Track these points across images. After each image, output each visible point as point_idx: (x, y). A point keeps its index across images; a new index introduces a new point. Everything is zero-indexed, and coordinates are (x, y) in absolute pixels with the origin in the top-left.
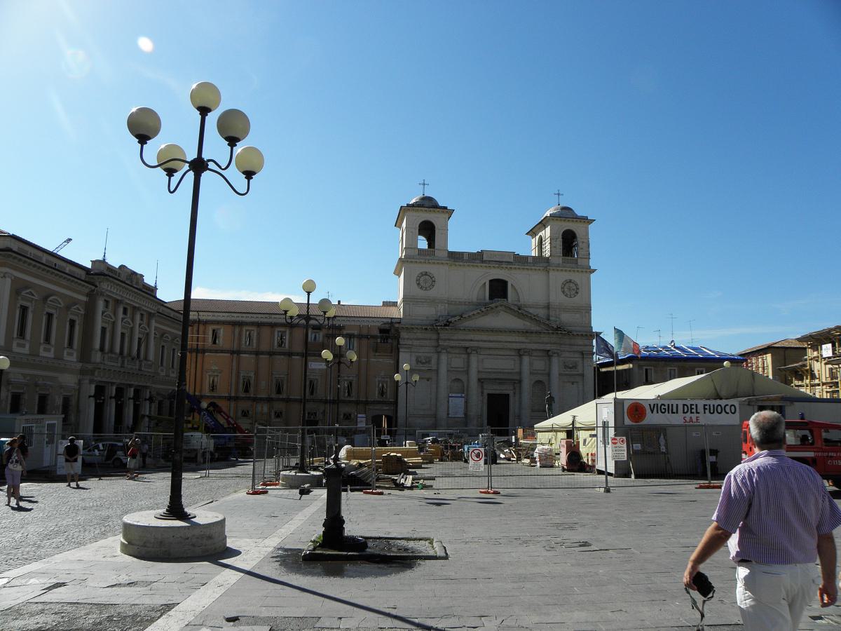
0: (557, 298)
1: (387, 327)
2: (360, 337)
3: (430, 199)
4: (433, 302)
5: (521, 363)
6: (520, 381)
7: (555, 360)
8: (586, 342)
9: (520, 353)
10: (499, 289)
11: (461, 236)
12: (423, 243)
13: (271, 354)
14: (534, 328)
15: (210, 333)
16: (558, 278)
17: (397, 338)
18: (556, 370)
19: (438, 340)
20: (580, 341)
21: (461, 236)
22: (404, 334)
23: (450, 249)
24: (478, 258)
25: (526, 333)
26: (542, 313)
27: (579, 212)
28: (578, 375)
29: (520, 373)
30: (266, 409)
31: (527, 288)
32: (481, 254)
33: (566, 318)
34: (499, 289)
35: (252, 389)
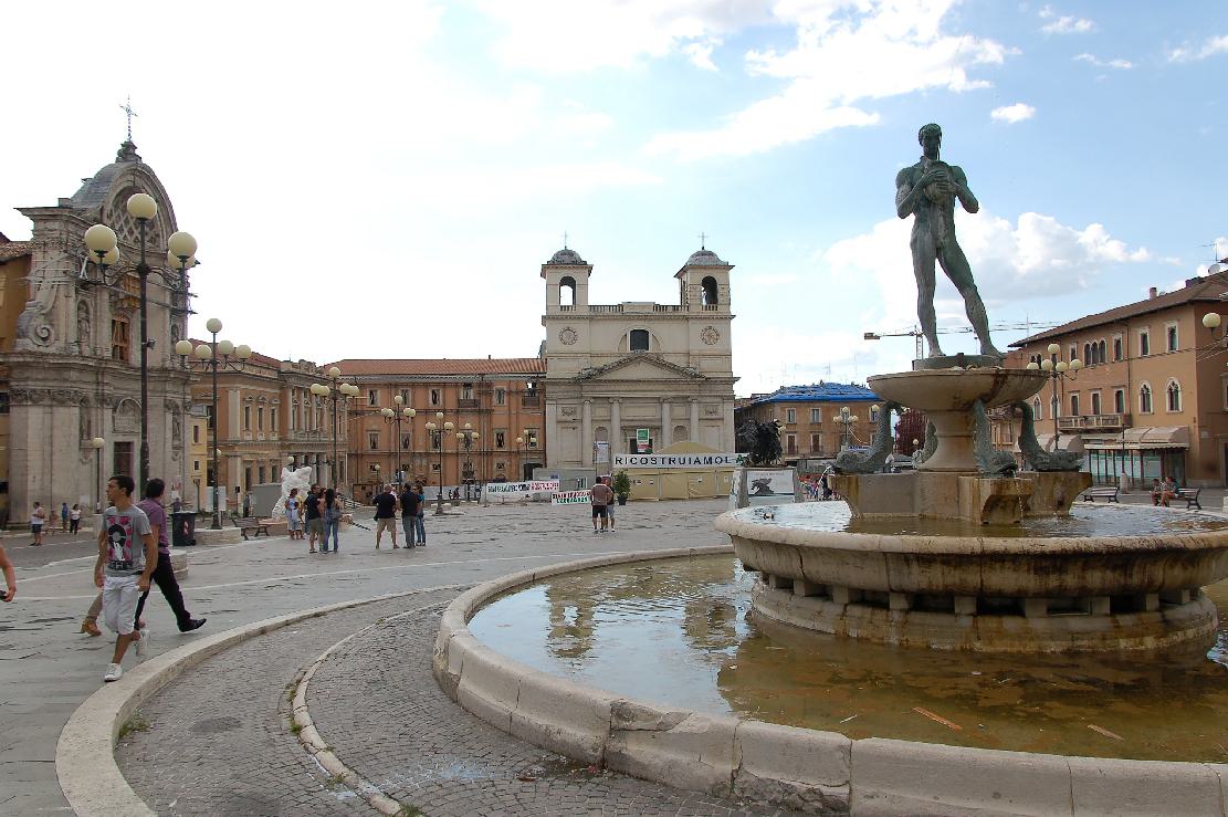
0: (697, 346)
2: (510, 393)
3: (571, 254)
4: (576, 355)
6: (660, 428)
7: (695, 407)
9: (660, 401)
10: (640, 339)
12: (566, 294)
14: (674, 376)
15: (368, 394)
16: (697, 328)
18: (695, 417)
20: (721, 387)
21: (600, 292)
24: (620, 312)
25: (666, 382)
26: (680, 362)
27: (723, 257)
28: (718, 419)
30: (424, 462)
31: (669, 341)
33: (708, 367)
34: (640, 339)
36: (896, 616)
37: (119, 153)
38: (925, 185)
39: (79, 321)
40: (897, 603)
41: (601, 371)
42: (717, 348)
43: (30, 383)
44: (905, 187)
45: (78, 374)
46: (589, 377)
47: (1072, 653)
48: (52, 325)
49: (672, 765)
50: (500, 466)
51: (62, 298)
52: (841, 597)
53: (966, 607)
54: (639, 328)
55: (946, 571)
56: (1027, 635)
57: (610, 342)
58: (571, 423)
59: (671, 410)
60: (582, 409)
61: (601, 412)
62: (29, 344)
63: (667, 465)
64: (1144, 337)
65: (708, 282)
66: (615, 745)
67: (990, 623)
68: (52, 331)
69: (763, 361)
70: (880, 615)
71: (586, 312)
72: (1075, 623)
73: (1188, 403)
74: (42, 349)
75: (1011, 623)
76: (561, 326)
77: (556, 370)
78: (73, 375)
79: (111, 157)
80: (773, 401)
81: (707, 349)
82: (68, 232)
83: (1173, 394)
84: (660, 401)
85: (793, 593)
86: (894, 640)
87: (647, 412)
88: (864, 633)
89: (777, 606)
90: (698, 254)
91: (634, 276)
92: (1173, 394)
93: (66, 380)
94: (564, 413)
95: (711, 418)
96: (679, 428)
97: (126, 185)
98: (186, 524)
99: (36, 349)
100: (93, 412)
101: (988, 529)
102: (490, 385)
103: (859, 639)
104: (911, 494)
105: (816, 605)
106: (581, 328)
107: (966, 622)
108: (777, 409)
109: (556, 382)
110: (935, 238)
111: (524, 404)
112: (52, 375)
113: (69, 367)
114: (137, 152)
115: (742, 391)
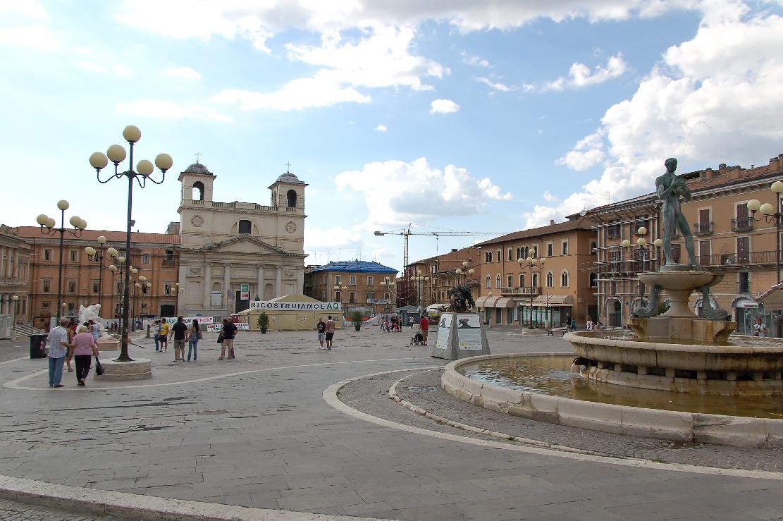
0: (282, 233)
1: (171, 249)
2: (154, 256)
3: (202, 167)
5: (258, 273)
6: (257, 284)
7: (279, 272)
8: (300, 260)
9: (257, 267)
10: (245, 226)
11: (221, 192)
12: (196, 194)
13: (90, 267)
14: (270, 252)
15: (44, 253)
16: (283, 222)
17: (178, 257)
18: (279, 278)
19: (205, 258)
21: (221, 192)
22: (182, 255)
23: (215, 200)
26: (272, 243)
29: (257, 279)
31: (264, 229)
32: (233, 204)
33: (288, 247)
34: (245, 226)
35: (76, 289)
36: (702, 382)
38: (675, 187)
40: (701, 376)
41: (219, 246)
42: (294, 235)
44: (662, 186)
46: (210, 249)
47: (774, 396)
49: (735, 438)
50: (144, 306)
52: (671, 374)
53: (732, 377)
54: (245, 219)
55: (733, 361)
56: (758, 388)
57: (225, 227)
58: (196, 278)
59: (264, 273)
60: (205, 270)
61: (218, 272)
63: (284, 308)
64: (550, 246)
65: (290, 194)
66: (698, 432)
67: (743, 383)
69: (323, 243)
70: (694, 382)
71: (209, 206)
72: (773, 383)
73: (573, 283)
75: (751, 383)
76: (192, 214)
77: (189, 243)
80: (328, 271)
81: (288, 235)
83: (565, 278)
84: (257, 267)
85: (637, 373)
86: (703, 392)
87: (248, 274)
88: (687, 390)
89: (628, 379)
90: (285, 175)
91: (243, 185)
92: (565, 278)
94: (192, 271)
95: (290, 281)
96: (269, 285)
98: (42, 343)
101: (715, 343)
102: (139, 251)
103: (685, 393)
104: (667, 328)
105: (657, 378)
106: (207, 217)
107: (734, 383)
108: (330, 275)
109: (187, 251)
110: (675, 211)
111: (164, 265)
115: (307, 262)
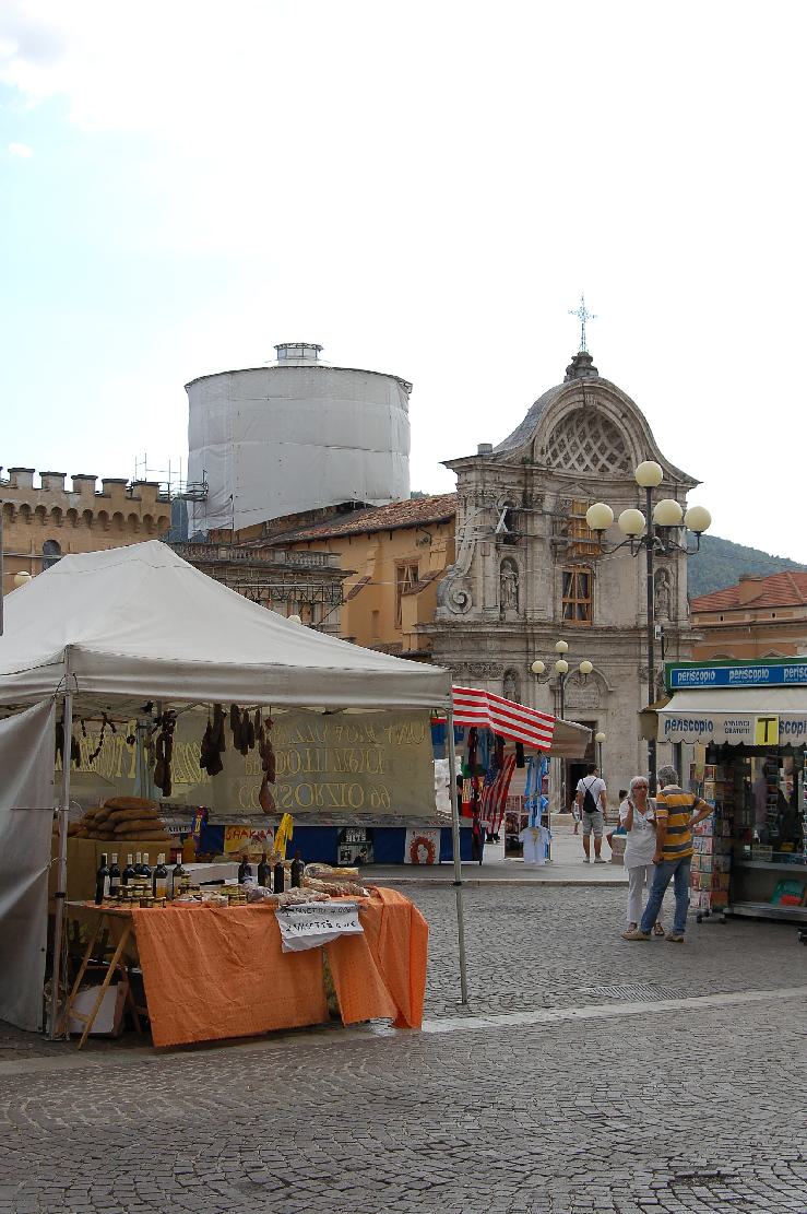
37: (568, 371)
39: (503, 582)
43: (446, 656)
45: (498, 643)
48: (470, 589)
51: (479, 557)
62: (446, 613)
68: (468, 596)
74: (459, 618)
78: (492, 645)
79: (557, 378)
82: (485, 482)
93: (482, 651)
97: (572, 407)
99: (453, 618)
100: (523, 686)
112: (471, 645)
113: (484, 636)
114: (592, 364)
